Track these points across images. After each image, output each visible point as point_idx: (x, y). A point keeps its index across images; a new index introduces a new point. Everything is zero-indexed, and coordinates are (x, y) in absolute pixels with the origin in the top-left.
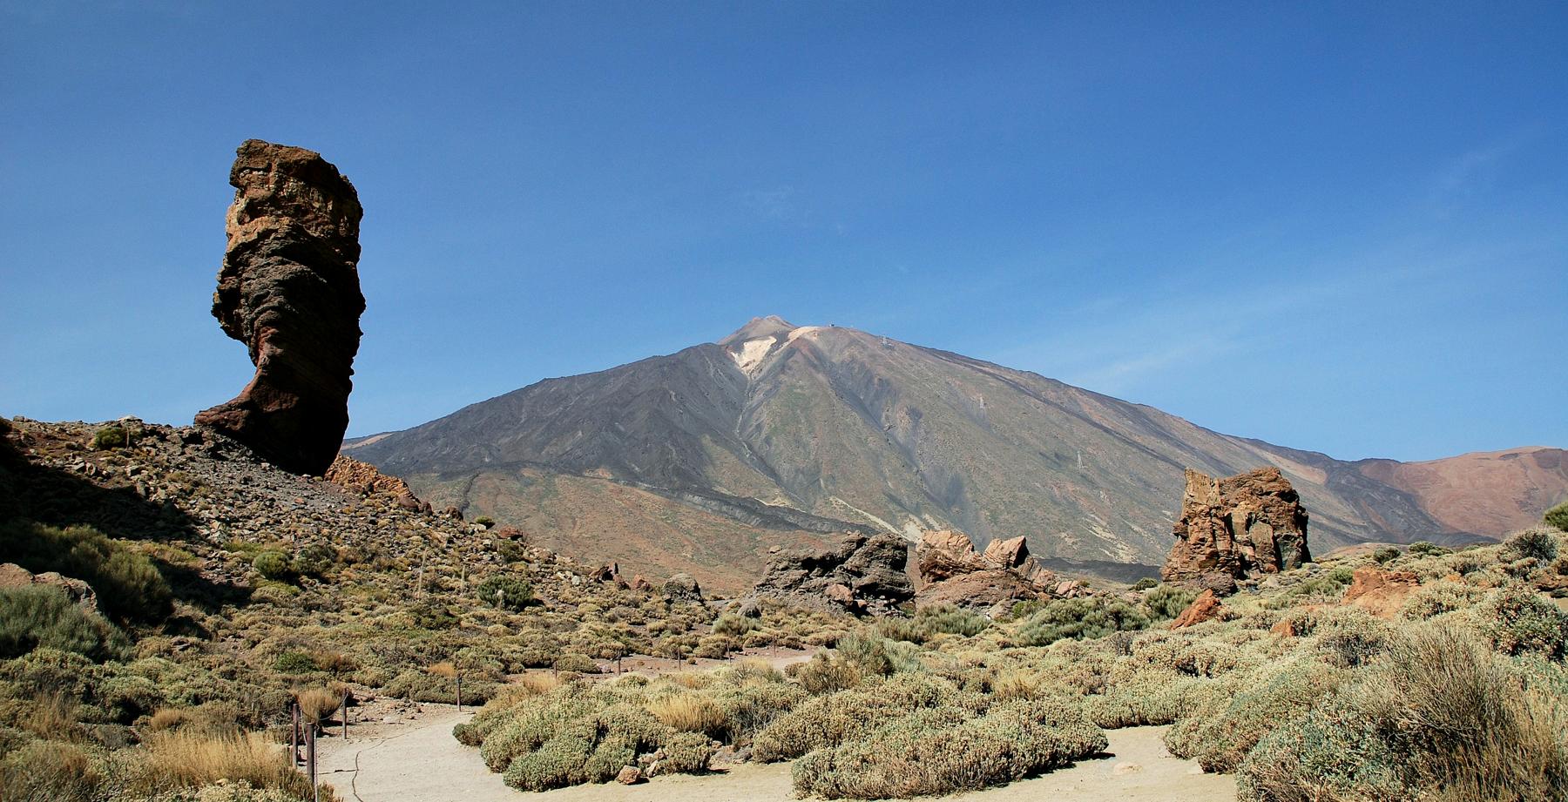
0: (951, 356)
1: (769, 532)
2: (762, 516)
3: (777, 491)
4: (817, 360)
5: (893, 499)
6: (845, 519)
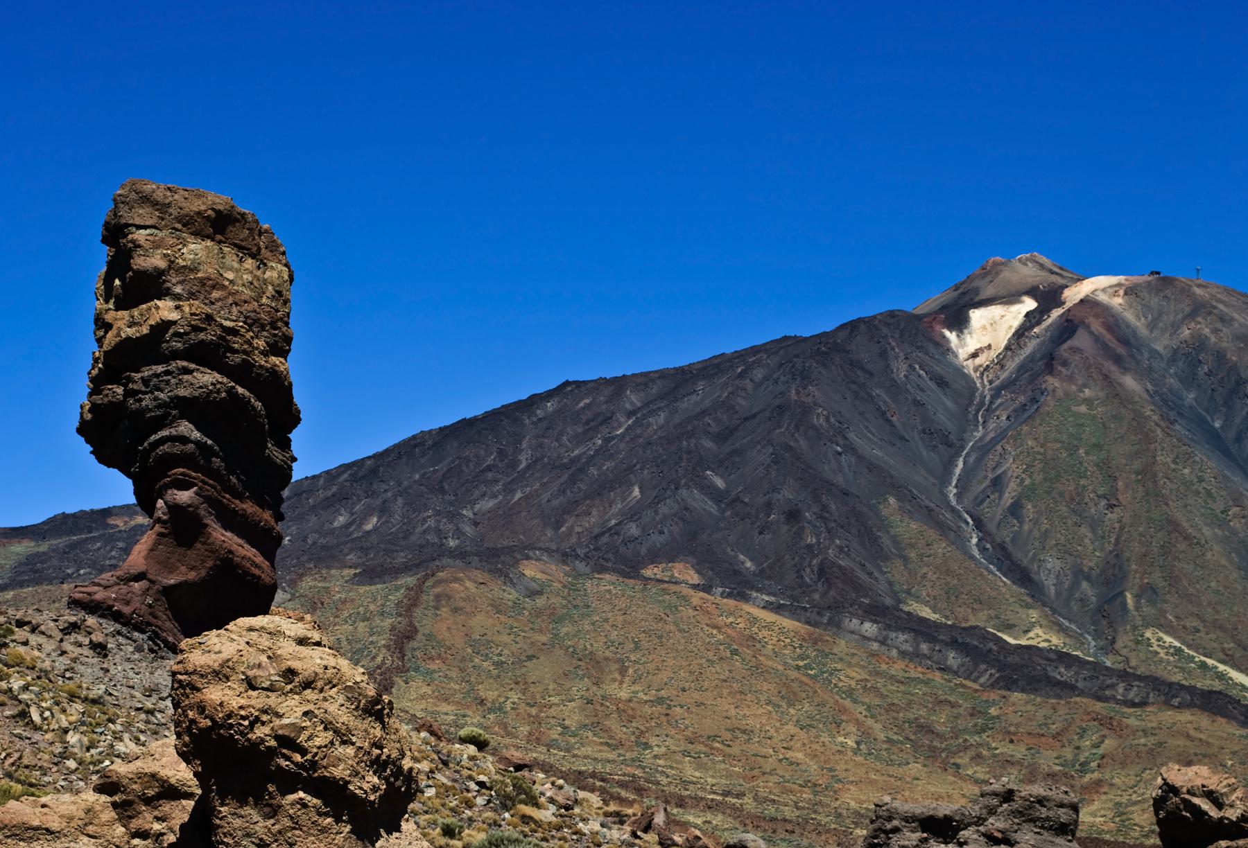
1: (1017, 696)
2: (1002, 667)
3: (1034, 615)
4: (1120, 344)
6: (1177, 677)
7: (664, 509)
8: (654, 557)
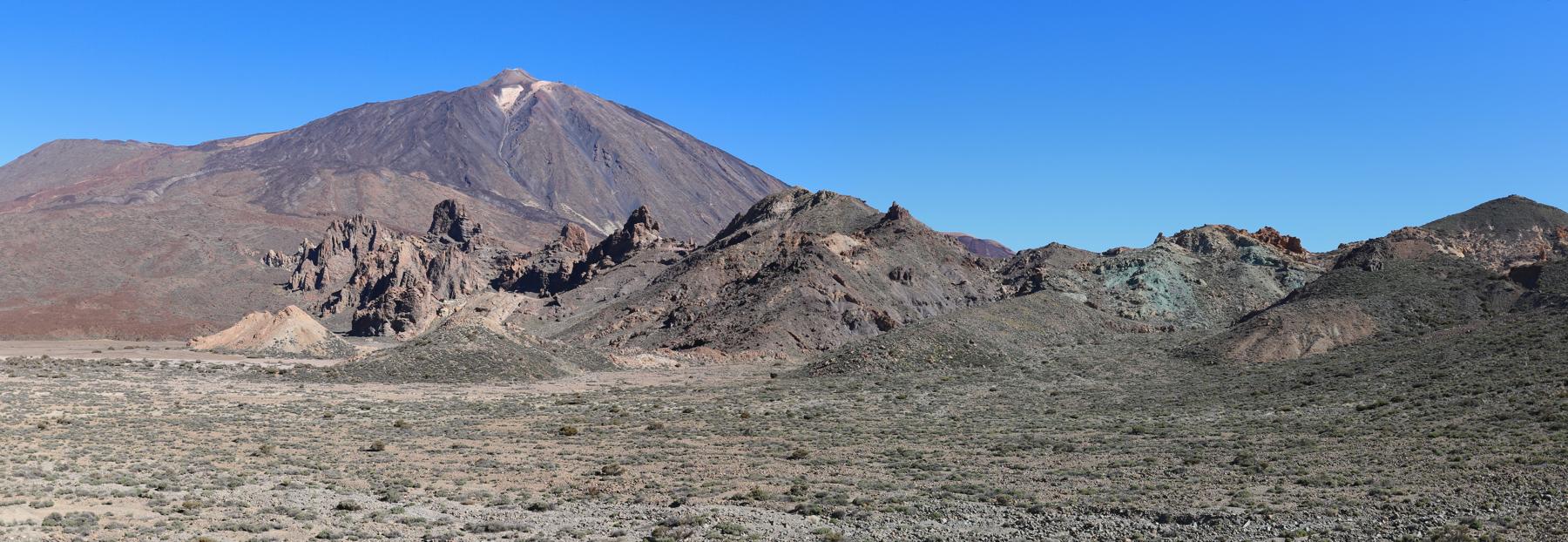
0: (636, 114)
4: (551, 108)
5: (598, 209)
7: (414, 153)
8: (413, 169)
